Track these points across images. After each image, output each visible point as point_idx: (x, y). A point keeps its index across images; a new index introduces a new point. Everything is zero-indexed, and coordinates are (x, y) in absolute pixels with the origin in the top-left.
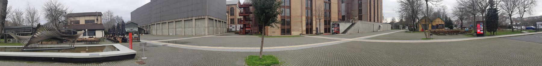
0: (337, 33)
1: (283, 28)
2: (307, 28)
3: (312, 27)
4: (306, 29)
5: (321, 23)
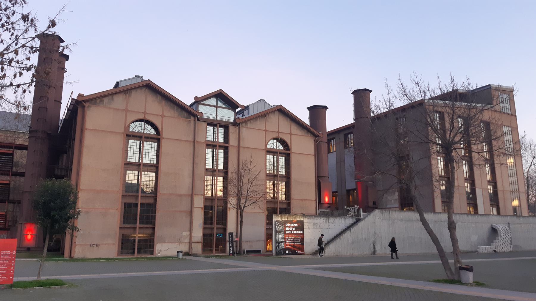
0: (293, 253)
2: (208, 232)
4: (204, 235)
5: (243, 220)
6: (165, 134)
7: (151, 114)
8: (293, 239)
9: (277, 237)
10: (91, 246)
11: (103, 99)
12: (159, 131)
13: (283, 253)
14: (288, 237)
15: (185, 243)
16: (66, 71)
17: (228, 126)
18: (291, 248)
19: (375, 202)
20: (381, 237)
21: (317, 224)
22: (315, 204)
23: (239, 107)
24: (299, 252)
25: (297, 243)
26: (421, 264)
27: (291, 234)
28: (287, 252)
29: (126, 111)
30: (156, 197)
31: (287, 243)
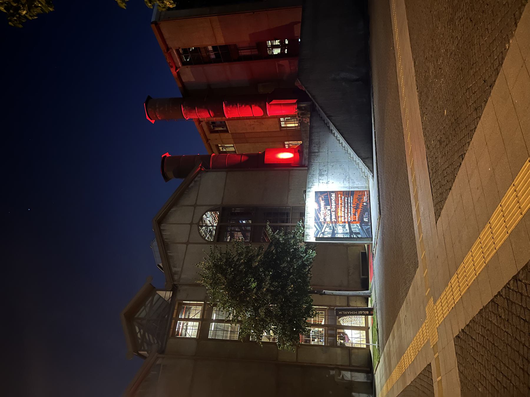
8: (345, 208)
9: (343, 237)
13: (368, 227)
18: (359, 212)
24: (365, 199)
27: (335, 211)
31: (351, 219)
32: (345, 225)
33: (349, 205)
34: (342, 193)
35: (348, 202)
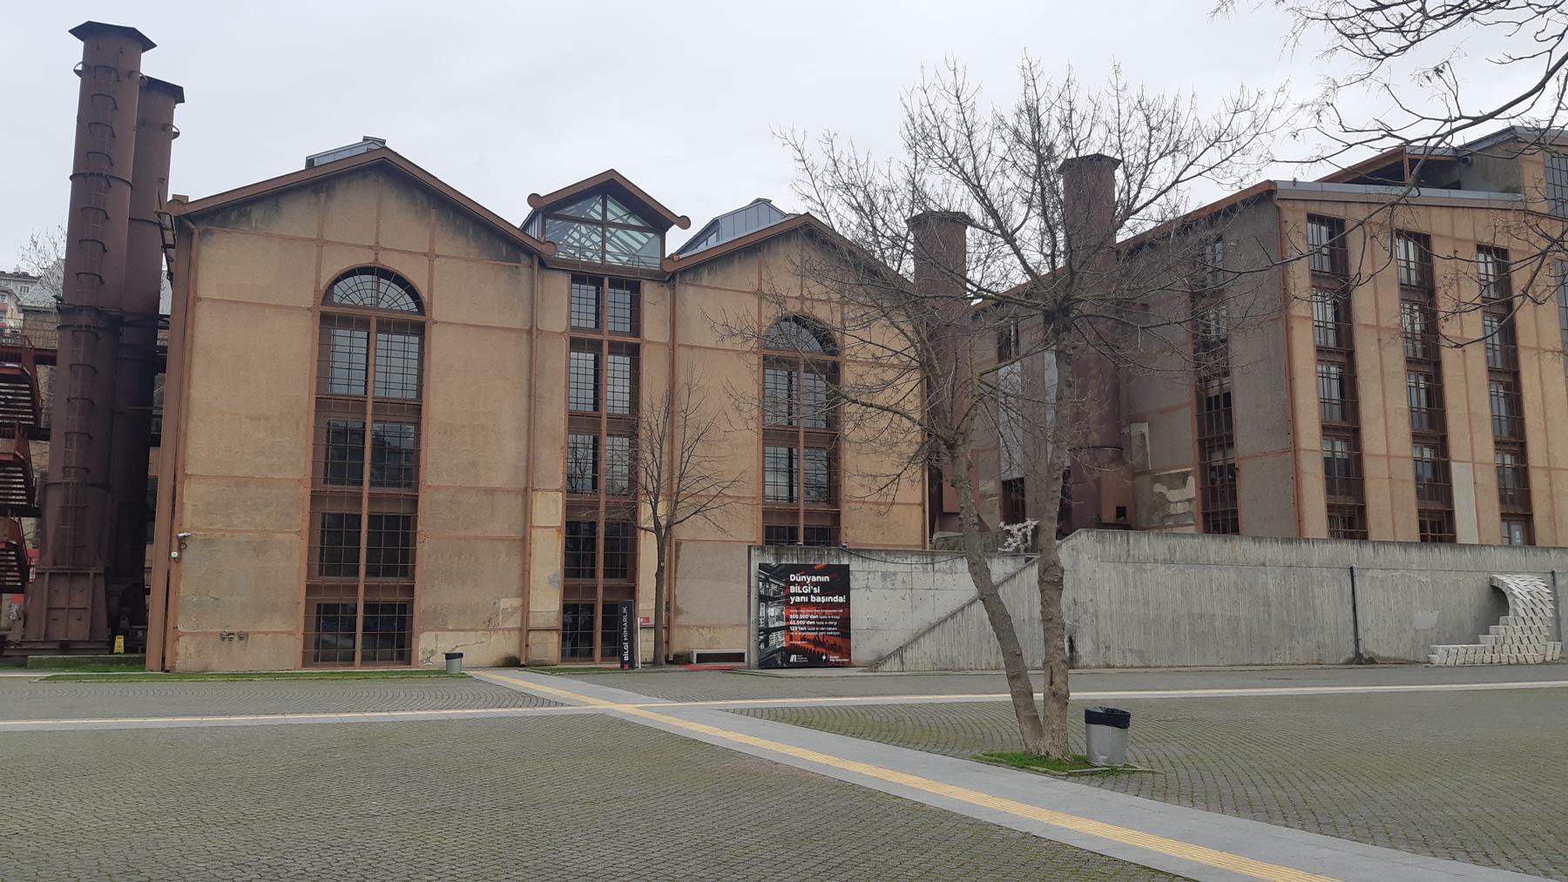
0: (814, 661)
1: (332, 599)
3: (632, 592)
4: (567, 608)
6: (439, 310)
7: (397, 251)
8: (816, 620)
9: (761, 615)
10: (223, 639)
11: (248, 209)
12: (421, 301)
13: (779, 662)
14: (799, 614)
15: (507, 633)
16: (177, 135)
17: (639, 283)
19: (1124, 508)
20: (1097, 617)
21: (895, 574)
22: (921, 514)
23: (673, 224)
24: (834, 658)
25: (826, 631)
26: (920, 705)
27: (809, 604)
28: (793, 658)
29: (321, 242)
30: (417, 496)
32: (782, 620)
33: (823, 629)
34: (846, 615)
35: (829, 626)
